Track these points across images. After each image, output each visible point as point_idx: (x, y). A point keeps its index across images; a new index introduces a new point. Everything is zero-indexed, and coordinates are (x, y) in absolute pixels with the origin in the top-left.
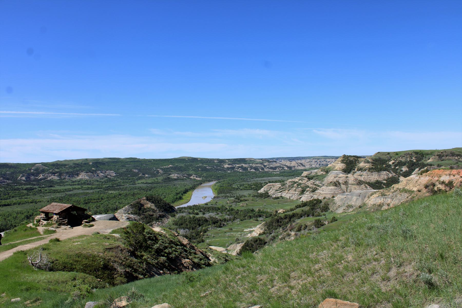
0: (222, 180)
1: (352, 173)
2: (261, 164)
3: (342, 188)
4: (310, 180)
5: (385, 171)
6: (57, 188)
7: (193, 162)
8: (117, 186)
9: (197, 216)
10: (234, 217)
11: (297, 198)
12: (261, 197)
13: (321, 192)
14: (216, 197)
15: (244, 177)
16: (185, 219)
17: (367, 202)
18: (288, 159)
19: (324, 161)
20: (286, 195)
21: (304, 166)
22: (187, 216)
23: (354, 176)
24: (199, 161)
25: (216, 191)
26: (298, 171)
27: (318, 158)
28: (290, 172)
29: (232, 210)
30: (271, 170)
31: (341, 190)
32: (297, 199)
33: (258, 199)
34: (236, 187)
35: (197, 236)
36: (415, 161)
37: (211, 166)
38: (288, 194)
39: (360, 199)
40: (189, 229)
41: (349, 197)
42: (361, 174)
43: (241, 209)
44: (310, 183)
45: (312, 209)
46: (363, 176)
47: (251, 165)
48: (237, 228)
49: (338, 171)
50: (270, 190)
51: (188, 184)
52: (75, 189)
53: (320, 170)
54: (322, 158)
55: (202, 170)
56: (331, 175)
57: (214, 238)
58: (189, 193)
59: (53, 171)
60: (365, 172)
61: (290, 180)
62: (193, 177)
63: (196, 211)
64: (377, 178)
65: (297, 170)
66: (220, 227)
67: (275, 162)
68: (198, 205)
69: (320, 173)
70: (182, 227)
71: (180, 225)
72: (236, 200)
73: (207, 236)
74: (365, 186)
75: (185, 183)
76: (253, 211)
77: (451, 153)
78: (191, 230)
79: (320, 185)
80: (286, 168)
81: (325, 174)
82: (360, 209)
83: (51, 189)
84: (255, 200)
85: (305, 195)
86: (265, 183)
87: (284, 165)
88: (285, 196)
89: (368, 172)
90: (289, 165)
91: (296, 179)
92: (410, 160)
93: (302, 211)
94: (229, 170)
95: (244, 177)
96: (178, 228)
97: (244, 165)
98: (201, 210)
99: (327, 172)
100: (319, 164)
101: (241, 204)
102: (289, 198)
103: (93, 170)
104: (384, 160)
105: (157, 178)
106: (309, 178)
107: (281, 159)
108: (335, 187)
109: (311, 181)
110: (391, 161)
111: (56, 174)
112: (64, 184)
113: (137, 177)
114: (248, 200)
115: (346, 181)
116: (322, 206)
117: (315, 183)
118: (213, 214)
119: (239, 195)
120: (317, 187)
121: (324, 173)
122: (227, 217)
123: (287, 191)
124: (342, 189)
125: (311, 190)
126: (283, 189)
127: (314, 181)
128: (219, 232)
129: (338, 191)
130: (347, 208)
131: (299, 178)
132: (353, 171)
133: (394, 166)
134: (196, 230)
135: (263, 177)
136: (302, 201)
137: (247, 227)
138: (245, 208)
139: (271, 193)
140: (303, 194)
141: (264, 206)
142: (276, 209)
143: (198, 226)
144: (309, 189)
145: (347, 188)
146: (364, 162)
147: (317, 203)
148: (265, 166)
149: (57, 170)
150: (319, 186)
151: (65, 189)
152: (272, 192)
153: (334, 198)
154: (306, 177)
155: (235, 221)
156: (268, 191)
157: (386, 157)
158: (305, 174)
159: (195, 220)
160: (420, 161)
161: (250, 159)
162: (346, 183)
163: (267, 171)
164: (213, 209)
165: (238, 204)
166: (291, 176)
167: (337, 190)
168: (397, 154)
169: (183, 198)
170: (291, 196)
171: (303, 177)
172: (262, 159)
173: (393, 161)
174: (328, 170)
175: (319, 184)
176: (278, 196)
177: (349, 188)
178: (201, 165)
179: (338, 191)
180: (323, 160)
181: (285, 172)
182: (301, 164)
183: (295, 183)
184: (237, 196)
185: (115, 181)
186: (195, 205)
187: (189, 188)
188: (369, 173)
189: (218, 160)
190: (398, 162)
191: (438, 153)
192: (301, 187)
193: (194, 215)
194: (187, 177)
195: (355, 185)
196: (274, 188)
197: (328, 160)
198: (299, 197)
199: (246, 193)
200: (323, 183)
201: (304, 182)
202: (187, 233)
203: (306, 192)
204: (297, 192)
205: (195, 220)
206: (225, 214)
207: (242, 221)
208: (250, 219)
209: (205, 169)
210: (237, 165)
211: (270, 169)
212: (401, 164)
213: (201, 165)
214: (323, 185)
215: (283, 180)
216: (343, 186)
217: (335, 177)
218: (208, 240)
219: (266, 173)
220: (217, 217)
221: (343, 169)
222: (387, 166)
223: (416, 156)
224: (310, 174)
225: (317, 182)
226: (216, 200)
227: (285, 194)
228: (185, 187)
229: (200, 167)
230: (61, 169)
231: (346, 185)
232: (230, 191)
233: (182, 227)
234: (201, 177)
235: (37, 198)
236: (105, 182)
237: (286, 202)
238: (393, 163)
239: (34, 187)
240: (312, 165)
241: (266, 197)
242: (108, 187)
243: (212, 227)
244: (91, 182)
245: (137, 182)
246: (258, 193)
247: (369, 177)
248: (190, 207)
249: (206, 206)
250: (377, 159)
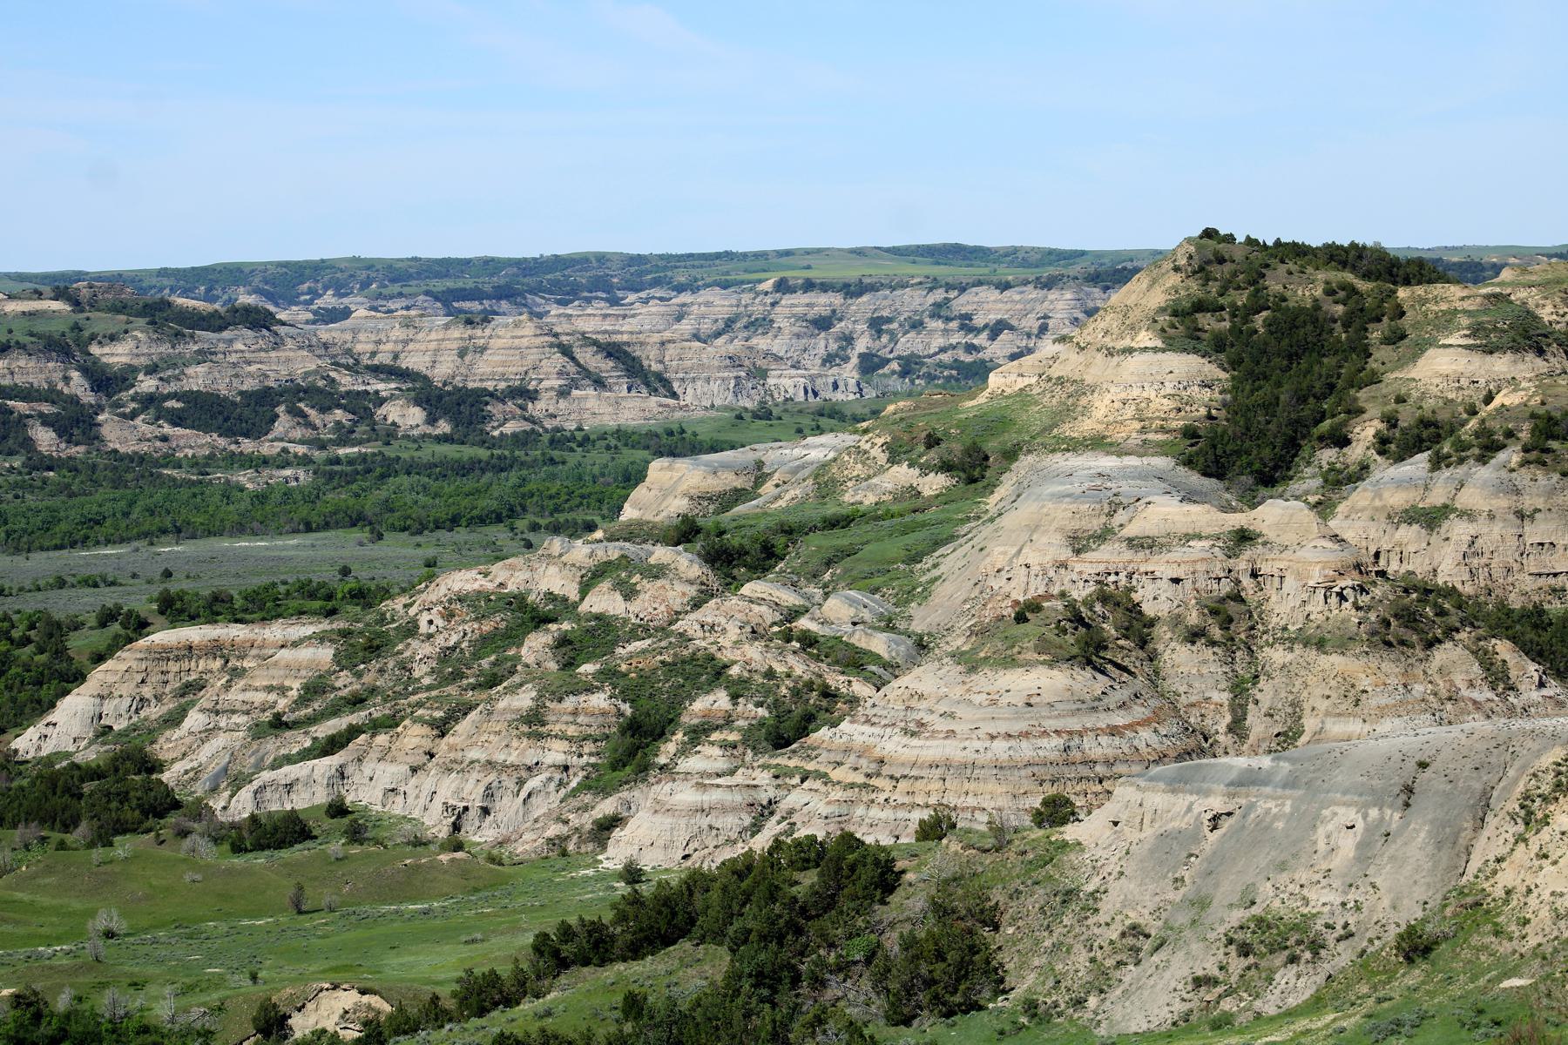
1: (1308, 481)
3: (1174, 684)
4: (732, 584)
11: (554, 830)
13: (894, 746)
17: (1507, 877)
18: (439, 285)
19: (938, 311)
21: (659, 383)
23: (1335, 524)
26: (573, 459)
27: (852, 274)
28: (464, 469)
30: (193, 442)
31: (1155, 719)
32: (558, 843)
38: (427, 781)
39: (1417, 838)
41: (1271, 805)
42: (1437, 497)
45: (760, 978)
49: (1119, 450)
50: (174, 719)
54: (904, 269)
60: (1484, 473)
61: (464, 581)
65: (559, 439)
67: (258, 320)
79: (879, 644)
80: (406, 416)
81: (944, 498)
82: (1414, 977)
85: (661, 789)
86: (107, 617)
87: (376, 370)
89: (1523, 477)
90: (443, 370)
93: (634, 1005)
100: (870, 364)
102: (443, 832)
107: (341, 290)
108: (1085, 681)
109: (747, 589)
115: (1226, 587)
116: (909, 943)
117: (804, 623)
120: (835, 680)
121: (934, 484)
123: (413, 736)
124: (1171, 706)
125: (752, 711)
126: (357, 701)
127: (789, 598)
129: (1114, 731)
130: (1237, 964)
131: (580, 552)
132: (1328, 455)
135: (87, 532)
136: (632, 874)
140: (644, 769)
141: (89, 949)
142: (259, 991)
144: (719, 700)
145: (1240, 691)
146: (1475, 331)
147: (826, 902)
148: (106, 382)
150: (855, 661)
152: (211, 754)
153: (1070, 832)
154: (685, 533)
156: (153, 732)
158: (666, 493)
163: (141, 459)
166: (482, 520)
167: (1103, 720)
170: (473, 794)
171: (636, 533)
172: (61, 286)
175: (860, 640)
176: (300, 801)
179: (1114, 731)
180: (914, 300)
181: (389, 468)
182: (614, 352)
192: (609, 675)
195: (1343, 643)
196: (235, 696)
197: (987, 305)
200: (921, 619)
201: (652, 602)
203: (683, 751)
204: (556, 753)
211: (177, 420)
214: (922, 646)
215: (362, 574)
217: (1079, 544)
219: (117, 483)
221: (1190, 433)
224: (739, 496)
227: (389, 773)
231: (1229, 644)
237: (409, 884)
240: (763, 374)
241: (131, 815)
247: (1535, 533)
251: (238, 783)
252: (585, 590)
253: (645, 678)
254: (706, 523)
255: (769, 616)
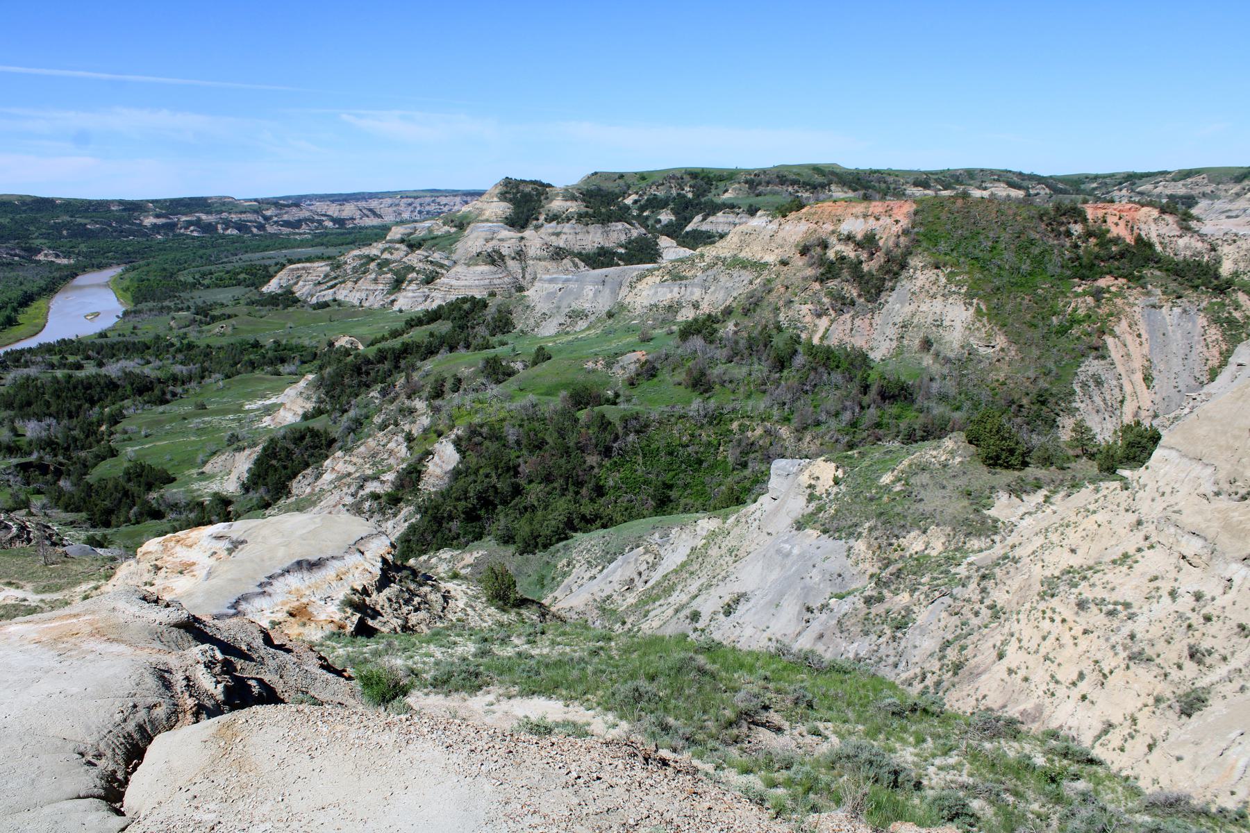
0: (141, 262)
1: (531, 227)
2: (257, 211)
4: (413, 251)
5: (619, 221)
7: (39, 210)
9: (80, 374)
10: (202, 367)
12: (273, 305)
13: (454, 282)
14: (131, 312)
15: (208, 252)
16: (39, 384)
20: (348, 294)
22: (42, 376)
24: (61, 205)
25: (129, 295)
29: (190, 346)
31: (508, 275)
33: (265, 309)
34: (191, 280)
35: (87, 436)
36: (690, 195)
37: (101, 223)
38: (354, 293)
40: (57, 416)
42: (559, 230)
43: (219, 344)
44: (415, 259)
46: (564, 237)
47: (224, 215)
48: (218, 403)
50: (296, 283)
51: (32, 279)
53: (440, 222)
55: (73, 235)
56: (475, 234)
57: (149, 439)
58: (40, 303)
60: (567, 225)
62: (46, 255)
63: (71, 359)
64: (600, 240)
66: (164, 401)
68: (74, 338)
69: (441, 229)
70: (31, 413)
71: (21, 407)
72: (198, 317)
73: (126, 437)
74: (573, 262)
75: (18, 276)
76: (256, 345)
77: (778, 177)
78: (65, 422)
79: (446, 262)
84: (258, 314)
85: (404, 293)
86: (277, 264)
88: (347, 299)
89: (576, 226)
91: (374, 250)
92: (678, 194)
94: (159, 233)
95: (208, 252)
96: (16, 416)
97: (204, 217)
98: (90, 353)
99: (462, 224)
101: (216, 328)
104: (612, 193)
106: (413, 246)
110: (630, 195)
114: (236, 316)
118: (131, 365)
119: (204, 302)
120: (438, 270)
121: (453, 230)
122: (178, 369)
123: (350, 284)
124: (509, 273)
125: (421, 277)
127: (426, 254)
128: (163, 417)
131: (381, 245)
132: (535, 222)
133: (638, 209)
134: (81, 417)
136: (401, 311)
137: (253, 396)
138: (233, 340)
139: (301, 290)
140: (400, 289)
141: (287, 331)
142: (327, 338)
143: (87, 405)
144: (414, 275)
145: (523, 269)
150: (442, 266)
154: (402, 241)
155: (207, 380)
157: (615, 184)
158: (396, 233)
159: (75, 388)
160: (704, 196)
161: (221, 198)
162: (520, 255)
164: (128, 350)
165: (205, 328)
168: (643, 177)
169: (20, 322)
170: (363, 296)
171: (391, 241)
172: (256, 200)
173: (634, 197)
174: (464, 222)
175: (442, 262)
176: (326, 299)
177: (529, 270)
178: (69, 219)
183: (371, 259)
184: (197, 307)
186: (64, 340)
187: (35, 289)
188: (579, 227)
189: (121, 202)
190: (648, 200)
191: (748, 177)
192: (391, 270)
193: (66, 371)
194: (23, 258)
195: (545, 259)
196: (309, 278)
198: (389, 300)
199: (224, 296)
200: (454, 257)
201: (397, 255)
202: (52, 429)
204: (381, 287)
205: (75, 388)
206: (170, 361)
207: (230, 377)
208: (252, 372)
209: (81, 233)
210: (184, 218)
212: (656, 204)
213: (66, 218)
216: (513, 265)
217: (487, 241)
218: (129, 449)
220: (147, 370)
221: (506, 218)
222: (620, 209)
223: (692, 182)
224: (411, 234)
225: (437, 256)
226: (133, 320)
227: (345, 292)
228: (24, 288)
229: (64, 225)
232: (171, 293)
233: (31, 413)
234: (73, 256)
237: (354, 315)
238: (635, 202)
243: (137, 403)
246: (262, 294)
247: (579, 237)
248: (48, 349)
249: (103, 341)
250: (592, 191)
251: (312, 296)
252: (382, 253)
253: (398, 271)
254: (406, 238)
255: (422, 257)
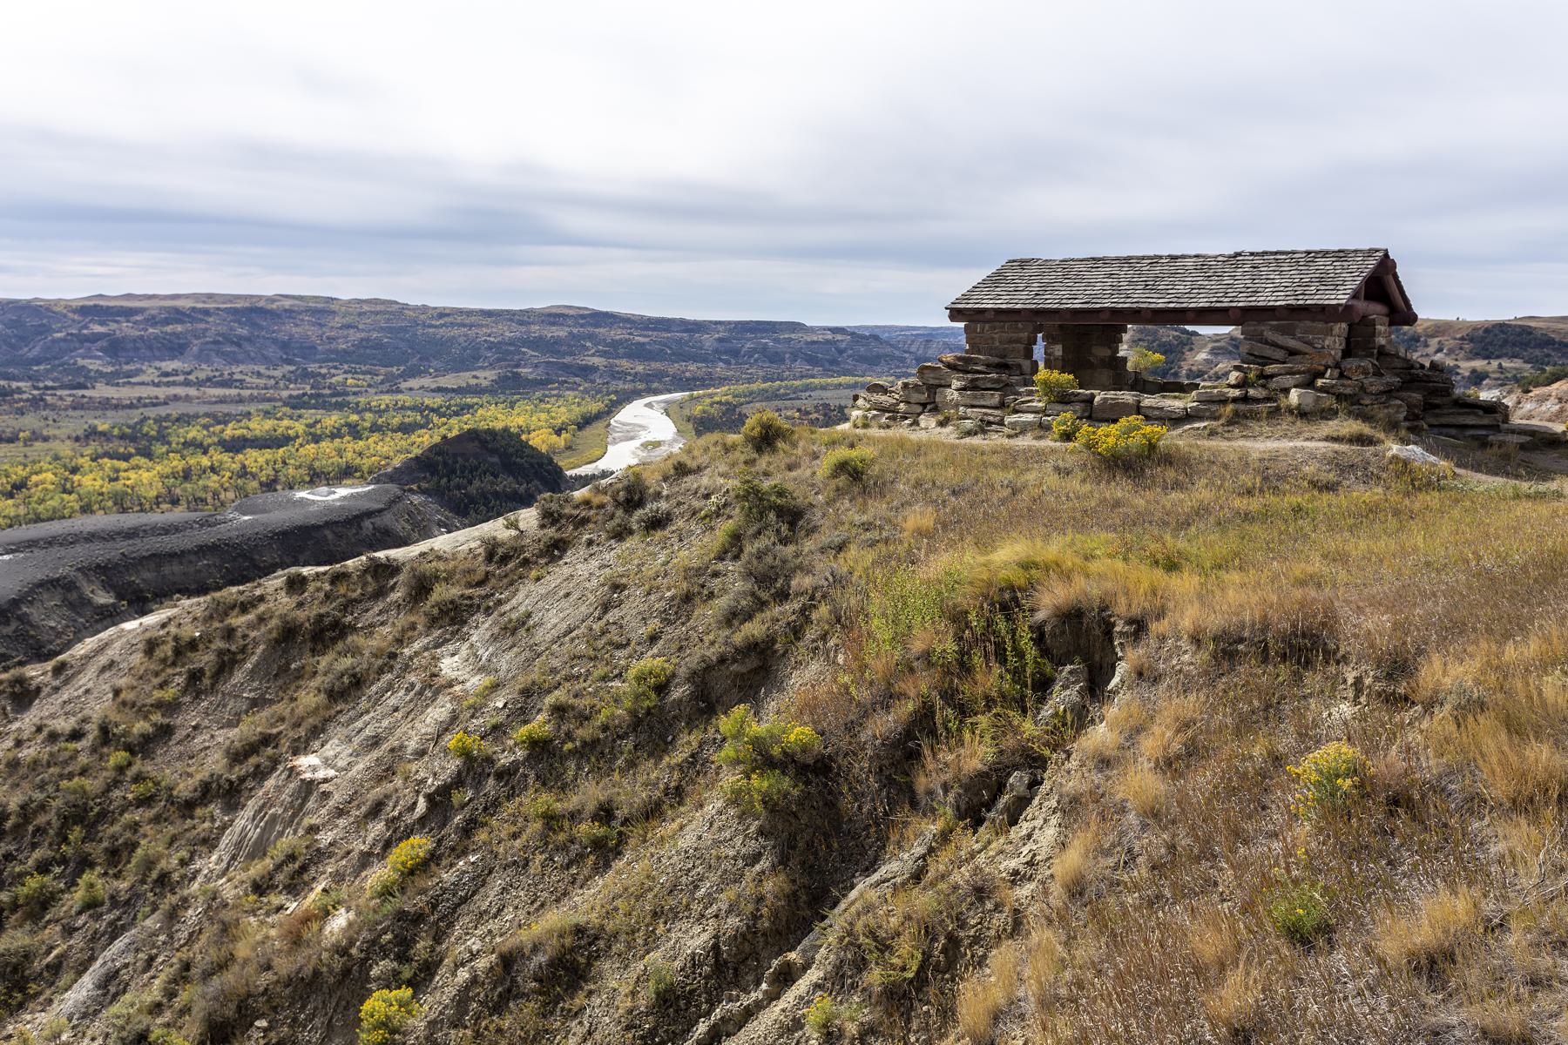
6: (102, 391)
7: (597, 326)
8: (333, 395)
52: (176, 398)
59: (85, 332)
83: (83, 396)
103: (240, 337)
105: (474, 373)
111: (99, 343)
112: (133, 380)
113: (402, 368)
149: (98, 329)
151: (140, 399)
185: (324, 376)
229: (620, 342)
230: (113, 326)
235: (30, 421)
236: (289, 380)
239: (15, 385)
242: (298, 397)
244: (236, 377)
245: (403, 385)
